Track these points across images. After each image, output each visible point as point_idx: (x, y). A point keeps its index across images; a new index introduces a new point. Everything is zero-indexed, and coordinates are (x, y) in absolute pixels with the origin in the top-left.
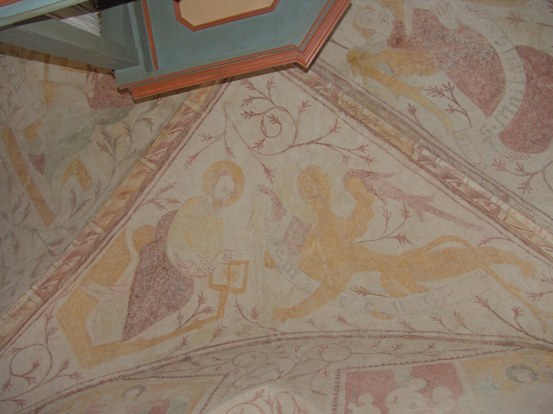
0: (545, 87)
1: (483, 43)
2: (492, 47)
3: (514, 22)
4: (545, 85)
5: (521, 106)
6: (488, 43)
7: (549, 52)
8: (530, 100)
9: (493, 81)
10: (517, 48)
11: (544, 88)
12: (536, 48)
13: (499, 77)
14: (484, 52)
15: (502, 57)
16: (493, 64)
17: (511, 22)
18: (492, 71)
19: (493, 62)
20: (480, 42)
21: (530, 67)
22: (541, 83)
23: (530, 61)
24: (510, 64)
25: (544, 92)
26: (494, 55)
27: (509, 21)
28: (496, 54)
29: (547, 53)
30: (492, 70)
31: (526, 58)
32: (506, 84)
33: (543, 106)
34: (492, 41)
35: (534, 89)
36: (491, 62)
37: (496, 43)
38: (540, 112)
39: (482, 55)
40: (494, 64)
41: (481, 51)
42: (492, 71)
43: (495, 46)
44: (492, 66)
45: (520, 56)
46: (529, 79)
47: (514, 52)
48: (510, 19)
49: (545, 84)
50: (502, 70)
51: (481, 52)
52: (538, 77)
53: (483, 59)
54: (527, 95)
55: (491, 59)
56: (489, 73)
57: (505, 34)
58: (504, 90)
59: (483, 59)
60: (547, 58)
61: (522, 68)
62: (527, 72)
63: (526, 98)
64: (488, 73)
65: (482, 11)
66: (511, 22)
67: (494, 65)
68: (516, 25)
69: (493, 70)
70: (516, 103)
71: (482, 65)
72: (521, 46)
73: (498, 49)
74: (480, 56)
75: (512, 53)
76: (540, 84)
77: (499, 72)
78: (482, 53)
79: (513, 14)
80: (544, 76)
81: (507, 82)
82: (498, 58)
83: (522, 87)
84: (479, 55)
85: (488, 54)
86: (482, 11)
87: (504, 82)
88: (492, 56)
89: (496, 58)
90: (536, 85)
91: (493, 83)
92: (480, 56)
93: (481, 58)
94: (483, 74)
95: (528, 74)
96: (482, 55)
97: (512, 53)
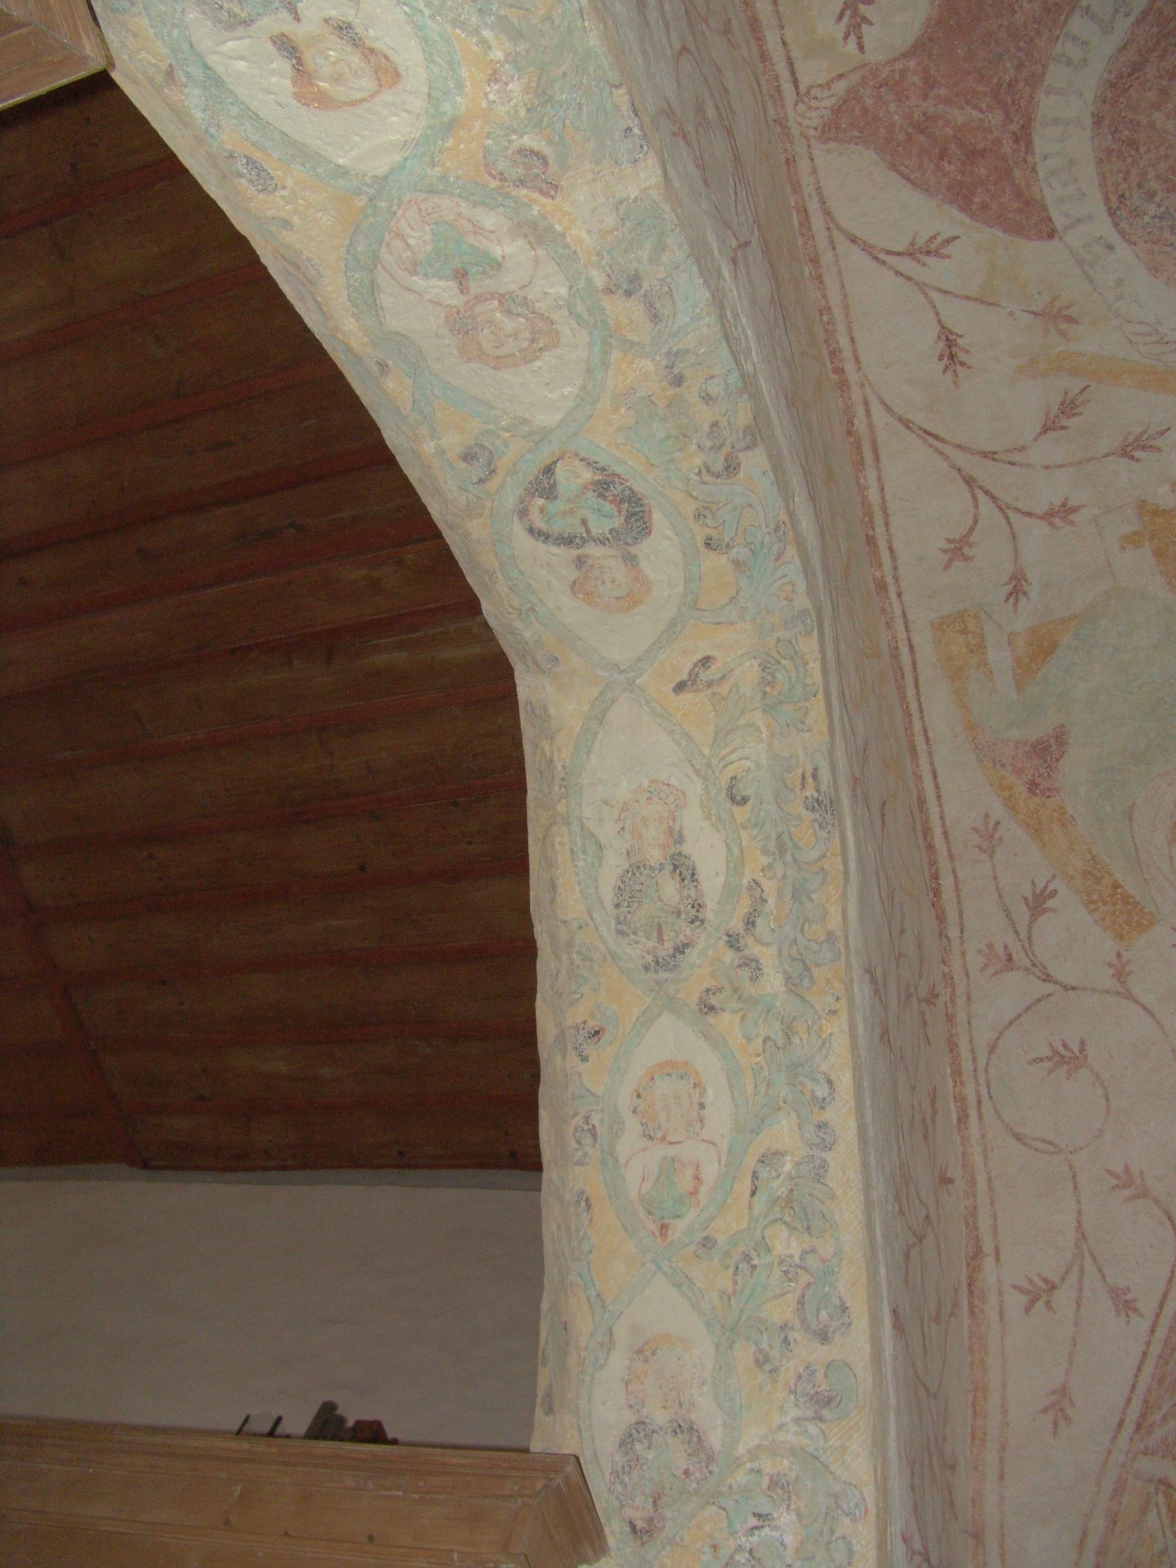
0: (981, 110)
1: (1149, 245)
2: (1122, 233)
3: (1060, 309)
4: (981, 116)
5: (1058, 38)
6: (1135, 244)
7: (967, 220)
8: (1027, 63)
9: (1131, 121)
10: (1051, 234)
11: (983, 106)
12: (1001, 235)
13: (1109, 137)
14: (1147, 219)
15: (1094, 204)
16: (1125, 180)
17: (1067, 307)
18: (1131, 156)
19: (1125, 186)
20: (1156, 248)
21: (1017, 173)
22: (993, 123)
23: (1019, 194)
24: (1076, 180)
25: (985, 93)
26: (1118, 208)
27: (1073, 312)
28: (1111, 213)
29: (971, 217)
30: (1129, 160)
31: (1027, 203)
32: (1093, 115)
33: (993, 44)
34: (1124, 251)
35: (1013, 101)
36: (1129, 188)
37: (1110, 247)
38: (1006, 23)
39: (1152, 209)
40: (1121, 181)
41: (1156, 220)
42: (1131, 156)
43: (1116, 239)
44: (1128, 172)
45: (1044, 208)
46: (1023, 137)
47: (1059, 221)
48: (1070, 320)
49: (981, 120)
50: (1100, 162)
51: (1154, 217)
52: (998, 142)
53: (1151, 195)
54: (1035, 80)
55: (1127, 195)
56: (1137, 150)
57: (1085, 272)
58: (1099, 94)
59: (1151, 195)
60: (972, 203)
61: (1042, 171)
62: (1029, 159)
63: (1040, 69)
64: (1142, 150)
65: (1145, 344)
66: (1067, 307)
67: (1121, 175)
68: (1053, 300)
69: (1125, 160)
70: (1074, 52)
71: (1158, 176)
72: (1040, 238)
73: (1104, 227)
74: (1159, 206)
75: (1067, 215)
76: (995, 118)
77: (1109, 152)
78: (1152, 213)
79: (1063, 334)
80: (981, 146)
81: (1088, 122)
82: (1107, 199)
83: (1047, 105)
84: (1162, 209)
85: (1135, 213)
86: (1145, 344)
87: (1098, 120)
88: (1122, 206)
89: (1113, 198)
90: (1007, 115)
91: (1131, 116)
92: (1159, 206)
93: (1157, 199)
94: (1157, 145)
95: (1026, 152)
96: (1152, 209)
97: (1067, 215)
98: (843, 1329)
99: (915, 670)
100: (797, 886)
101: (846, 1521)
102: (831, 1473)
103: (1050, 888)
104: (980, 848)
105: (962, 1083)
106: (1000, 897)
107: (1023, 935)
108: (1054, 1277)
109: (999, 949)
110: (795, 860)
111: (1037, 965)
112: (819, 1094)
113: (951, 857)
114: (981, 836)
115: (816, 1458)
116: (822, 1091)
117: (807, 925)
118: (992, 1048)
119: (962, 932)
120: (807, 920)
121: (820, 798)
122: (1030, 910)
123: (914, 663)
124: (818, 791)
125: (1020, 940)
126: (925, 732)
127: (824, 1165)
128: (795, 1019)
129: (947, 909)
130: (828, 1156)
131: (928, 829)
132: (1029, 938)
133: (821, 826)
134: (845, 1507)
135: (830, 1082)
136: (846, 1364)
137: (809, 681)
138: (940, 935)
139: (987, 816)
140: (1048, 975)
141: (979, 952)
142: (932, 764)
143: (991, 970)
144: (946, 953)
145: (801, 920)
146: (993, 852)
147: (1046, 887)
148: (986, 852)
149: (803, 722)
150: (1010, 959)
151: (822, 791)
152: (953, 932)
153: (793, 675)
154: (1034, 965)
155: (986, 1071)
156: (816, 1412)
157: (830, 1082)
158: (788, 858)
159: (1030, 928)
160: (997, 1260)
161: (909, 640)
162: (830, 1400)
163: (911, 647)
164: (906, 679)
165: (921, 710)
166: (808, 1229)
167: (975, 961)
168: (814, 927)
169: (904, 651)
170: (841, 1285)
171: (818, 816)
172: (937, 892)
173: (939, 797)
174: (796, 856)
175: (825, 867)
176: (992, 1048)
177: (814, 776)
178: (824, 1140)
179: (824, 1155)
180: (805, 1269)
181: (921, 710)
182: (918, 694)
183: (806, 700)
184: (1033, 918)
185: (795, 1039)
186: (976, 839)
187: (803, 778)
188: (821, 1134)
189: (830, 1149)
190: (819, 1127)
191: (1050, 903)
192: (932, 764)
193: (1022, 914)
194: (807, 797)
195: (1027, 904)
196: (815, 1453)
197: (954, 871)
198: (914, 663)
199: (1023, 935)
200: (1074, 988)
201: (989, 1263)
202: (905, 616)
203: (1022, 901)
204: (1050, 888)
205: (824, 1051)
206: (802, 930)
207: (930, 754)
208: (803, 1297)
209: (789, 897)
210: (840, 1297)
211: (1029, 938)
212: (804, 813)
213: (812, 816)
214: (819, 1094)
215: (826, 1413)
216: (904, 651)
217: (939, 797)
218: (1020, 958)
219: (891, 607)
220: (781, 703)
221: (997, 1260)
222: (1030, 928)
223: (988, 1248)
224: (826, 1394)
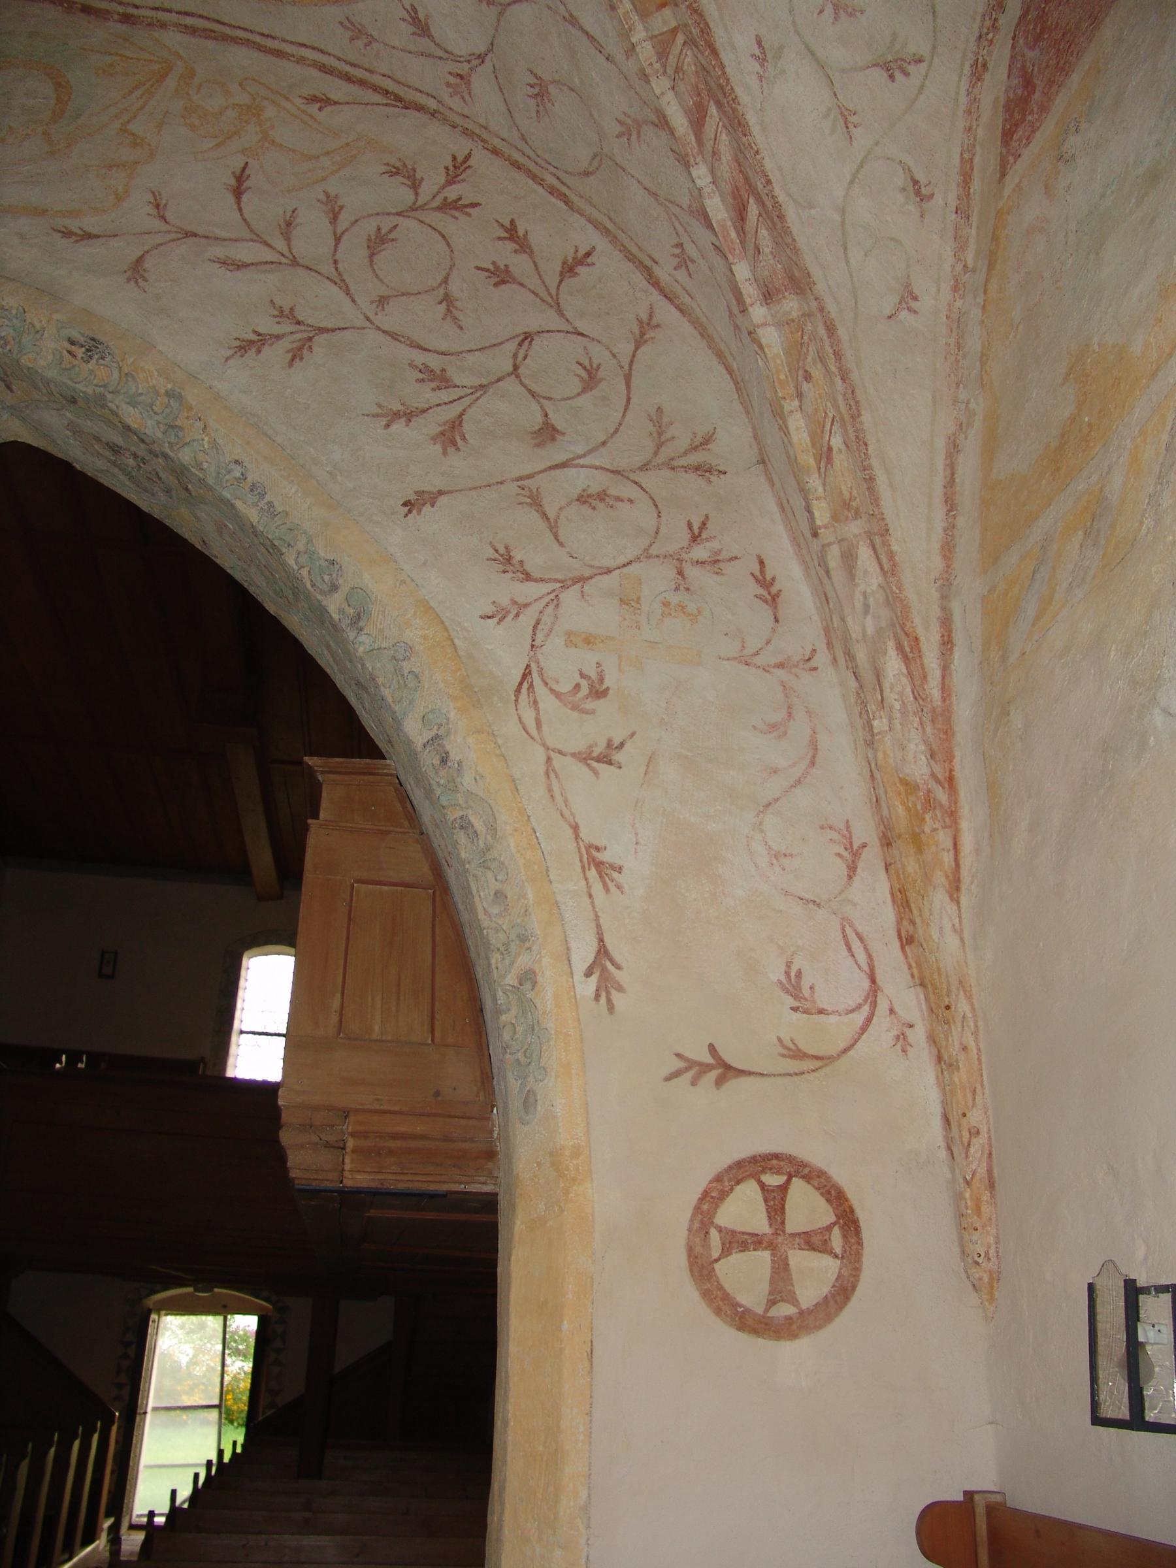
98: (340, 573)
99: (208, 19)
100: (128, 400)
101: (405, 664)
102: (385, 648)
103: (409, 8)
104: (366, 45)
105: (542, 180)
106: (410, 52)
107: (442, 54)
108: (675, 241)
109: (452, 80)
110: (112, 392)
111: (469, 58)
112: (238, 475)
113: (371, 72)
114: (357, 38)
115: (372, 650)
116: (237, 473)
117: (154, 407)
118: (523, 138)
119: (435, 98)
120: (151, 406)
121: (87, 347)
122: (424, 36)
123: (201, 17)
124: (82, 346)
125: (447, 59)
126: (263, 35)
127: (270, 504)
128: (195, 457)
129: (412, 99)
130: (267, 498)
131: (346, 75)
132: (447, 52)
133: (103, 358)
134: (401, 658)
135: (236, 462)
136: (353, 589)
137: (14, 311)
138: (433, 116)
139: (341, 23)
140: (479, 56)
141: (451, 96)
142: (292, 43)
143: (467, 97)
144: (447, 121)
145: (149, 409)
146: (371, 36)
147: (408, 12)
148: (371, 42)
149: (38, 332)
150: (461, 77)
151: (83, 343)
152: (432, 104)
153: (7, 322)
154: (469, 62)
155: (538, 156)
156: (357, 628)
157: (236, 462)
158: (109, 396)
159: (437, 45)
160: (656, 263)
161: (179, 13)
162: (359, 614)
163: (186, 14)
164: (216, 29)
165: (245, 29)
166: (289, 545)
167: (455, 103)
168: (158, 403)
169: (189, 21)
170: (322, 554)
171: (96, 357)
172: (398, 98)
173: (322, 51)
174: (110, 390)
175: (126, 372)
176: (523, 138)
177: (73, 343)
178: (259, 493)
179: (265, 501)
180: (303, 567)
181: (245, 29)
182: (230, 26)
183: (25, 321)
184: (430, 36)
185: (205, 465)
186: (360, 44)
187: (70, 352)
188: (256, 492)
189: (265, 493)
190: (252, 490)
191: (421, 16)
192: (292, 43)
193: (424, 44)
194: (82, 358)
195: (419, 35)
196: (371, 648)
197: (384, 76)
198: (201, 17)
199: (442, 54)
200: (492, 44)
201: (656, 270)
202: (156, 9)
203: (416, 37)
204: (409, 8)
205: (221, 452)
206: (155, 413)
207: (283, 40)
208: (312, 581)
209: (132, 408)
210: (326, 560)
211: (447, 52)
212: (90, 366)
213: (93, 361)
214: (238, 475)
215: (361, 624)
216: (189, 21)
217: (322, 51)
218: (464, 68)
219: (147, 17)
220: (20, 342)
221: (656, 263)
222: (437, 45)
223: (648, 263)
224: (355, 614)
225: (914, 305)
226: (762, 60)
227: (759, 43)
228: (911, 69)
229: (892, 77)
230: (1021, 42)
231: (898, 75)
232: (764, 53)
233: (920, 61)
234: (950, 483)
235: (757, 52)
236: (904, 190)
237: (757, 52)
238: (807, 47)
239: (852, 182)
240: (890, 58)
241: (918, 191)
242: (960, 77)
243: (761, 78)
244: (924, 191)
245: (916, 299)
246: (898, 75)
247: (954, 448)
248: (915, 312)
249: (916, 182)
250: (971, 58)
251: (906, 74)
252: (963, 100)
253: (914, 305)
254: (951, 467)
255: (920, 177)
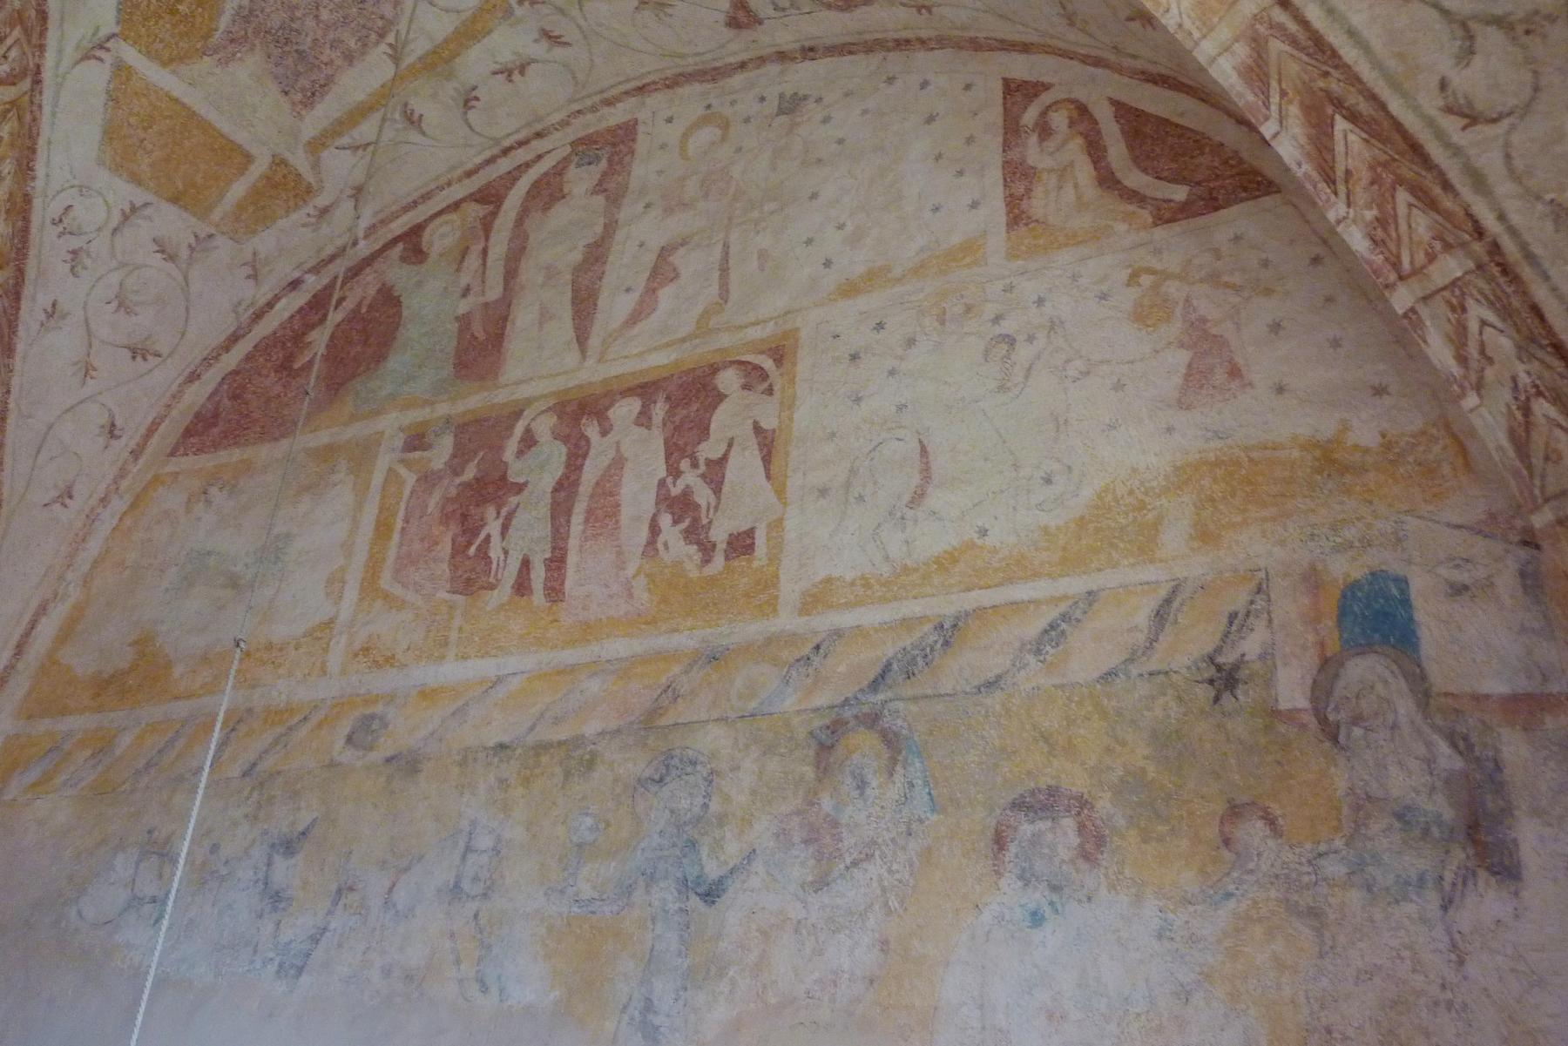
225: (68, 501)
226: (50, 316)
227: (54, 305)
228: (150, 358)
229: (134, 358)
230: (225, 387)
231: (139, 359)
232: (54, 313)
233: (159, 356)
234: (27, 634)
235: (50, 310)
236: (103, 427)
237: (50, 310)
238: (86, 320)
239: (68, 411)
240: (140, 346)
241: (112, 431)
242: (179, 375)
243: (42, 325)
244: (116, 432)
245: (71, 497)
246: (139, 359)
247: (43, 609)
248: (66, 506)
249: (113, 425)
250: (193, 367)
251: (145, 359)
252: (174, 388)
253: (68, 501)
254: (33, 625)
255: (118, 423)
